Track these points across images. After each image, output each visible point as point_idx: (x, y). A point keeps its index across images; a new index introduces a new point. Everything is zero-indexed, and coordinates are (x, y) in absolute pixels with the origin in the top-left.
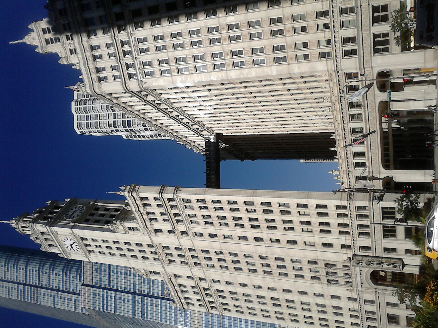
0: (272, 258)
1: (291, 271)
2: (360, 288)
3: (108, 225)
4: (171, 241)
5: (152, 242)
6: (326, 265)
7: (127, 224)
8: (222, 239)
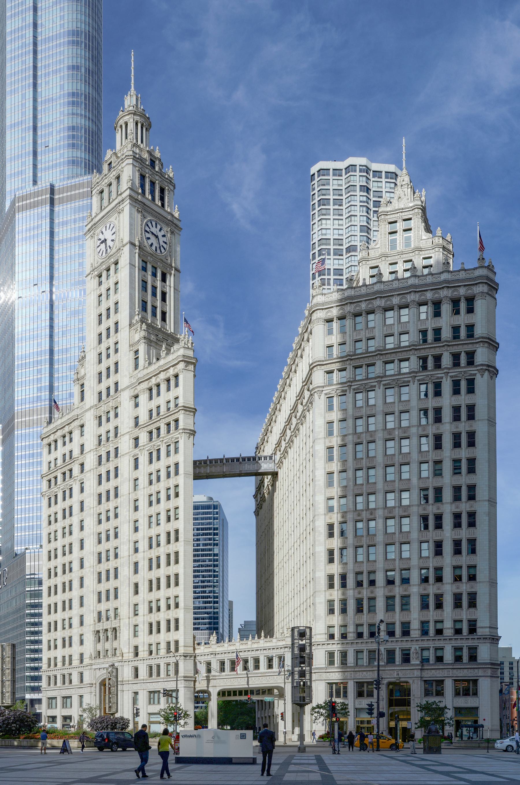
0: (116, 563)
1: (104, 587)
2: (94, 667)
3: (138, 315)
4: (125, 422)
5: (123, 390)
6: (115, 629)
7: (142, 348)
8: (133, 497)
